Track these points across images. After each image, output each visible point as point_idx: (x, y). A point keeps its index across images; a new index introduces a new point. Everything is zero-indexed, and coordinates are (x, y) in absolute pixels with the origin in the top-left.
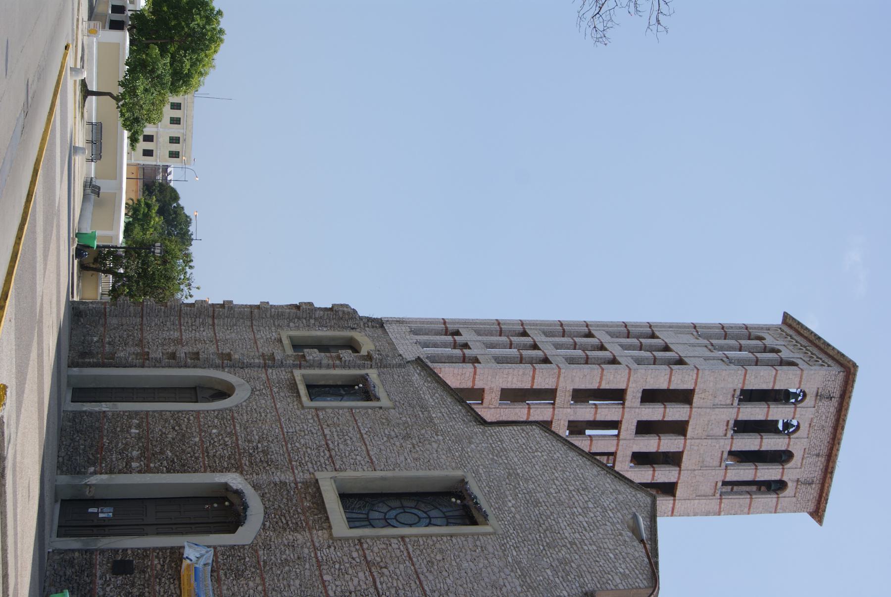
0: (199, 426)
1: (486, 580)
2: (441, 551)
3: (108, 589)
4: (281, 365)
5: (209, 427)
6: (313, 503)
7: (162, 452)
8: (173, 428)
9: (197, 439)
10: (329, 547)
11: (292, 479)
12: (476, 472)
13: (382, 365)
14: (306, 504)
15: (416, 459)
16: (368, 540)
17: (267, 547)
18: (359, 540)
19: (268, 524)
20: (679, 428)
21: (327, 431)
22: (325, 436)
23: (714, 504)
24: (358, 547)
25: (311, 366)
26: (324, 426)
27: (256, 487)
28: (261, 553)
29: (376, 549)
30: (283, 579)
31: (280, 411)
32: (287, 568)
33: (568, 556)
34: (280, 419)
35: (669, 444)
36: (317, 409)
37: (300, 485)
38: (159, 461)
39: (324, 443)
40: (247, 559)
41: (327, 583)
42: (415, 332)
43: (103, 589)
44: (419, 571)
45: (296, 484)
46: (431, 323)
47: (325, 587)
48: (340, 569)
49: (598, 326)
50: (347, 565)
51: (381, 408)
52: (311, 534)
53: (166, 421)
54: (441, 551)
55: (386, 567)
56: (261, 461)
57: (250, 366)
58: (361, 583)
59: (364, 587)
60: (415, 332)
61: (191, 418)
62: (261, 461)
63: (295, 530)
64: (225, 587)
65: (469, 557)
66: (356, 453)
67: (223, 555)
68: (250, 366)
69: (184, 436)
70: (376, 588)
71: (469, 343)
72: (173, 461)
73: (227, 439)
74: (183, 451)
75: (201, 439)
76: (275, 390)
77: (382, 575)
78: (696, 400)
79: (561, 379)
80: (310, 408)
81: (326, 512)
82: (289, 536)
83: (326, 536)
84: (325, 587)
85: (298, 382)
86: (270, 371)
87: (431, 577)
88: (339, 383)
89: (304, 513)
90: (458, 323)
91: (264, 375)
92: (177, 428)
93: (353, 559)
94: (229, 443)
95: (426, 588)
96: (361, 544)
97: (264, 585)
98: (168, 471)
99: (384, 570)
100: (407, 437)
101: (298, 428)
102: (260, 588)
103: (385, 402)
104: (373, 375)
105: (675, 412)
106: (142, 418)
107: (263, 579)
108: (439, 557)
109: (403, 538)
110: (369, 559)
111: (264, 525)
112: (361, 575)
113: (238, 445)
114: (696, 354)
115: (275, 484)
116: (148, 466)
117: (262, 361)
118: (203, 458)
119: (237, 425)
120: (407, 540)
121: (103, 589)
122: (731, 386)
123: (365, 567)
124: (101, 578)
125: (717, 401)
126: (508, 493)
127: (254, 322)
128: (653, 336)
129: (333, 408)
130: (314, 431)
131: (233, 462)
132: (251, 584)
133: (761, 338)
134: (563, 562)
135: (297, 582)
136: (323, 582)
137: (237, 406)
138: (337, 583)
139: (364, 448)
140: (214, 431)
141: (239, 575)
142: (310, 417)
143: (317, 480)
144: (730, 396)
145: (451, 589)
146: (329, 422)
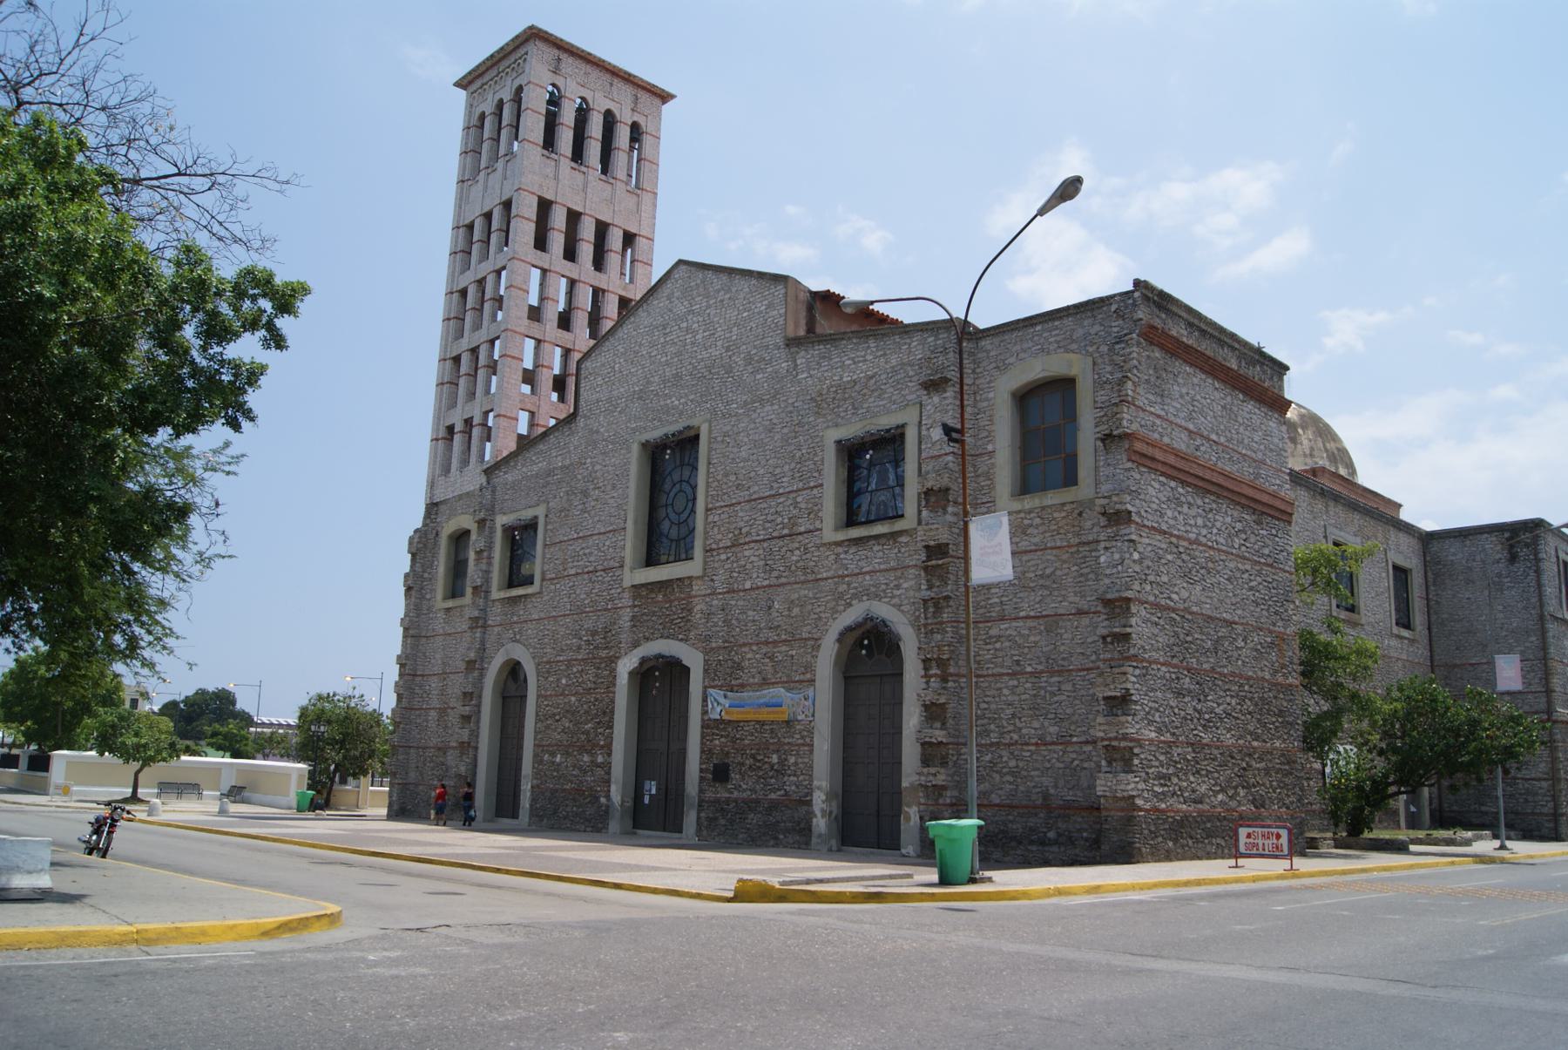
0: (556, 696)
1: (763, 436)
2: (726, 475)
3: (744, 787)
4: (484, 610)
6: (660, 592)
7: (587, 733)
8: (557, 721)
9: (573, 699)
10: (712, 580)
11: (628, 610)
12: (634, 430)
13: (491, 510)
14: (660, 597)
15: (614, 487)
16: (708, 543)
17: (708, 639)
18: (707, 551)
19: (680, 636)
20: (574, 217)
21: (573, 572)
22: (577, 574)
23: (646, 197)
24: (715, 553)
25: (487, 581)
26: (566, 574)
27: (636, 645)
28: (714, 645)
29: (720, 537)
30: (746, 626)
31: (542, 615)
32: (733, 622)
33: (742, 356)
34: (554, 617)
35: (587, 231)
36: (543, 579)
38: (597, 736)
39: (586, 576)
40: (721, 658)
41: (754, 586)
42: (446, 470)
43: (745, 790)
44: (747, 498)
45: (635, 606)
46: (435, 457)
47: (758, 588)
48: (739, 573)
49: (453, 281)
50: (735, 565)
51: (547, 516)
52: (695, 596)
53: (548, 727)
54: (726, 475)
55: (740, 529)
56: (604, 638)
57: (483, 642)
58: (756, 553)
59: (761, 552)
60: (446, 470)
61: (546, 703)
62: (604, 638)
63: (690, 611)
64: (751, 680)
65: (735, 450)
66: (601, 545)
68: (483, 642)
69: (567, 711)
70: (764, 540)
71: (466, 417)
72: (598, 723)
73: (575, 670)
74: (586, 712)
76: (515, 618)
77: (748, 533)
78: (549, 196)
79: (518, 329)
80: (541, 585)
81: (671, 580)
82: (697, 617)
83: (699, 582)
84: (758, 588)
85: (508, 595)
86: (490, 622)
87: (756, 488)
88: (509, 554)
90: (438, 424)
91: (496, 629)
92: (557, 717)
93: (728, 558)
94: (580, 668)
95: (767, 494)
96: (712, 550)
97: (751, 644)
98: (611, 727)
99: (744, 530)
100: (585, 493)
101: (566, 600)
102: (754, 648)
103: (540, 511)
104: (501, 520)
105: (559, 219)
106: (543, 751)
107: (744, 645)
108: (733, 478)
109: (707, 510)
110: (729, 544)
111: (681, 640)
112: (747, 553)
113: (583, 660)
114: (497, 187)
115: (634, 626)
116: (602, 747)
117: (479, 630)
119: (558, 658)
120: (710, 506)
121: (745, 790)
122: (539, 157)
123: (739, 549)
124: (732, 793)
125: (551, 175)
126: (662, 403)
127: (423, 634)
128: (470, 227)
129: (543, 563)
130: (571, 584)
131: (603, 665)
132: (749, 656)
133: (482, 117)
134: (749, 360)
135: (750, 613)
136: (752, 589)
137: (534, 658)
138: (755, 576)
139: (595, 538)
140: (564, 681)
141: (739, 667)
142: (553, 587)
143: (633, 586)
144: (548, 161)
145: (771, 470)
146: (561, 568)
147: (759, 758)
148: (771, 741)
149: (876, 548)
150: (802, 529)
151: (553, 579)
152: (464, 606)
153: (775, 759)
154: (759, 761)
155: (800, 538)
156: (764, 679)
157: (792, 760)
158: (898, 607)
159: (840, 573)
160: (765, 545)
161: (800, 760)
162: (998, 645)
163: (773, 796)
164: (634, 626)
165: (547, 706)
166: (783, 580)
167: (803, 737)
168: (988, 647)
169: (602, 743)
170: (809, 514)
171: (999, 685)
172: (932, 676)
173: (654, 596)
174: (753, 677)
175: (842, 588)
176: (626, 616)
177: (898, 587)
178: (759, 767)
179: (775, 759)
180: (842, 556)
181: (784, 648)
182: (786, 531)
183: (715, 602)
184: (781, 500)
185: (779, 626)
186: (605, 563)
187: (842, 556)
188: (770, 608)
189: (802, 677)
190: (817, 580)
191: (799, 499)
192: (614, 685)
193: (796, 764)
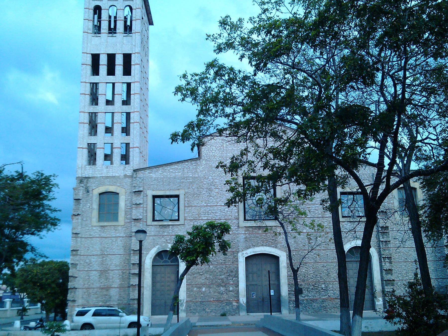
7: (222, 279)
21: (206, 218)
27: (248, 248)
37: (246, 233)
103: (181, 193)
106: (192, 287)
121: (310, 296)
147: (316, 286)
148: (321, 280)
151: (192, 220)
153: (323, 286)
154: (316, 287)
155: (327, 218)
156: (315, 261)
157: (331, 286)
162: (399, 254)
163: (323, 297)
168: (396, 254)
169: (231, 283)
171: (401, 265)
172: (386, 262)
174: (311, 260)
178: (316, 289)
179: (323, 286)
181: (324, 252)
182: (320, 216)
184: (317, 206)
186: (226, 217)
189: (332, 261)
192: (238, 261)
193: (332, 287)
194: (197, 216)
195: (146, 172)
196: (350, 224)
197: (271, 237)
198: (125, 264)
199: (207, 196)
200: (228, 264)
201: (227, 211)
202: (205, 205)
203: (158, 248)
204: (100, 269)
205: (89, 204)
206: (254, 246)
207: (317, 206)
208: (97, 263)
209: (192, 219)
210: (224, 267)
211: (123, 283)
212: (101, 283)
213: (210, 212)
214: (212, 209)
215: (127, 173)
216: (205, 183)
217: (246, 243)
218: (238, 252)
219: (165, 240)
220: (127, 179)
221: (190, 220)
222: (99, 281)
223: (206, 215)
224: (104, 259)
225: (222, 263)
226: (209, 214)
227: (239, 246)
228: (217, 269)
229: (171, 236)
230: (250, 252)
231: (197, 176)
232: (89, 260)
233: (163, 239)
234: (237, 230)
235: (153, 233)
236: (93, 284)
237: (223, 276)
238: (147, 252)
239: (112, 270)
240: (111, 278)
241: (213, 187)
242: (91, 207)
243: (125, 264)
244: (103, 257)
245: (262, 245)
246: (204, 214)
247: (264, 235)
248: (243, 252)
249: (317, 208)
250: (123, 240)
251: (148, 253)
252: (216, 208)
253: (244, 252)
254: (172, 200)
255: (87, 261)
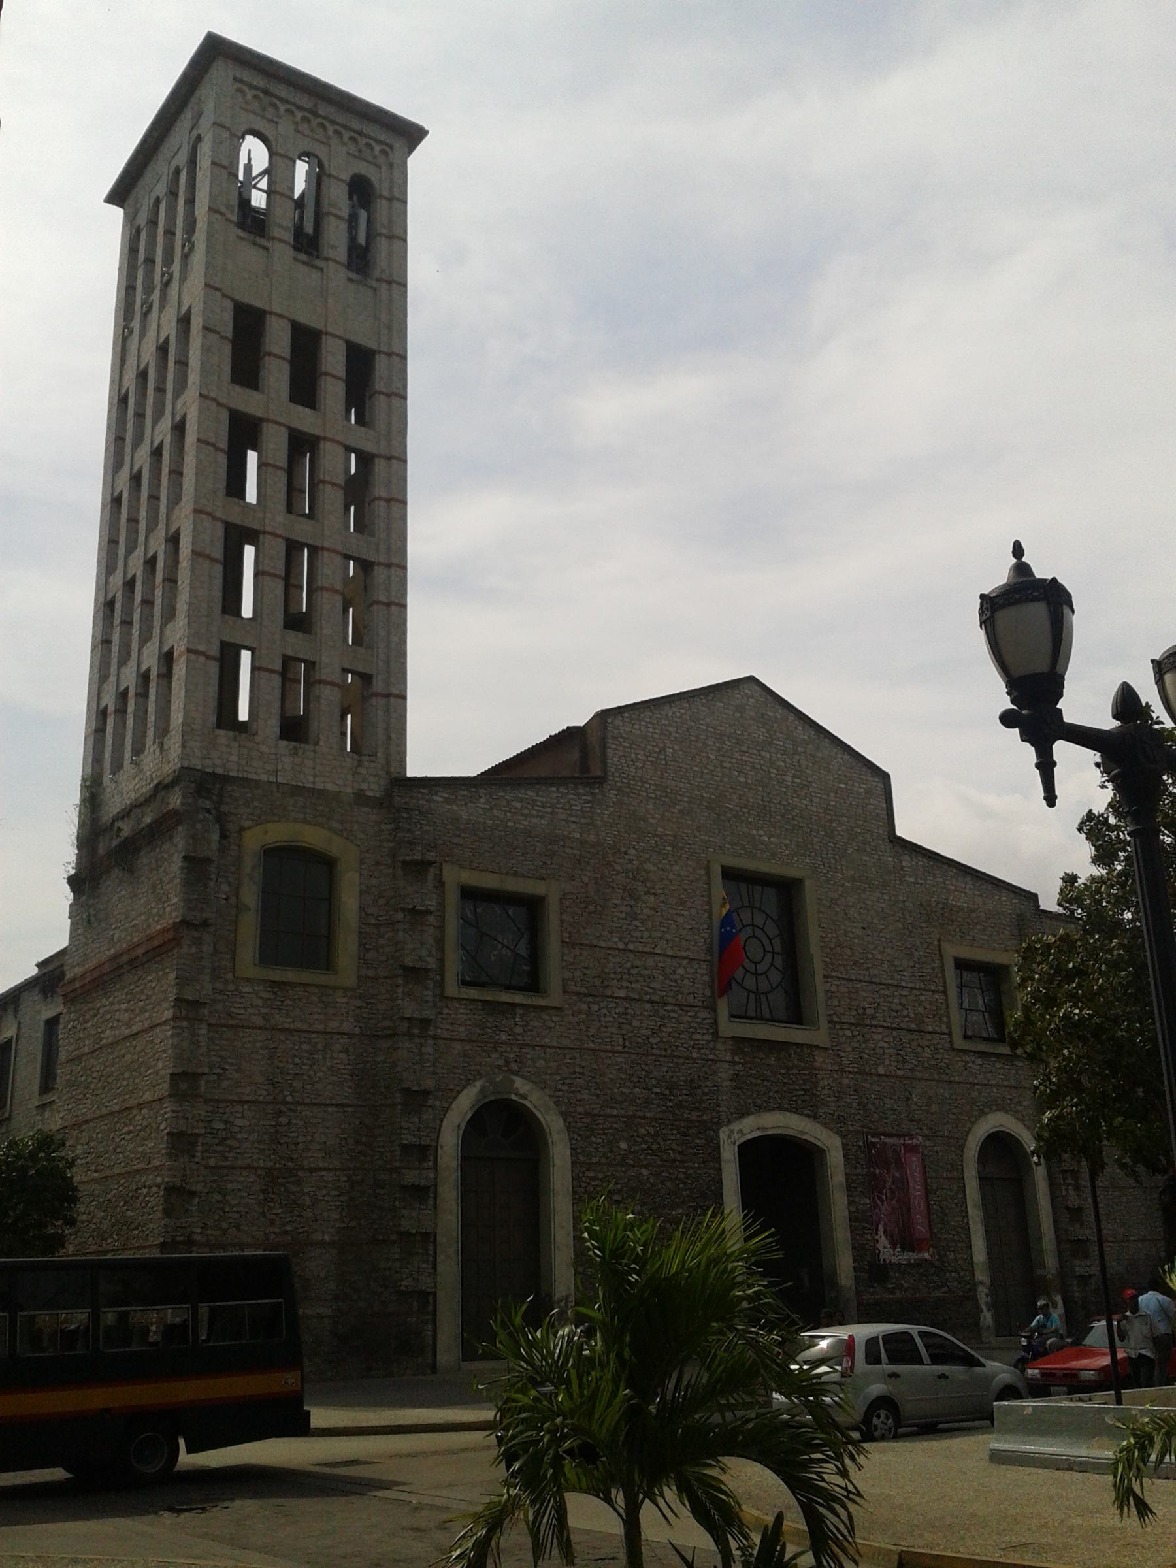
3: (906, 1285)
5: (611, 1151)
9: (645, 1172)
14: (772, 1061)
19: (806, 1112)
21: (622, 993)
27: (743, 1114)
29: (841, 1010)
32: (870, 1106)
37: (737, 1059)
43: (906, 1290)
61: (591, 1174)
67: (855, 1168)
75: (645, 1167)
77: (873, 1017)
89: (788, 1068)
111: (808, 1116)
112: (875, 1037)
113: (656, 1119)
115: (736, 1088)
118: (687, 1168)
119: (608, 1111)
123: (866, 1030)
124: (894, 1293)
142: (585, 1007)
143: (733, 1037)
149: (998, 1065)
150: (930, 1029)
152: (335, 988)
157: (952, 1257)
158: (1022, 1120)
159: (971, 1080)
160: (895, 1033)
161: (959, 1256)
163: (938, 1294)
164: (736, 1088)
165: (594, 1179)
166: (918, 1074)
167: (958, 1234)
170: (934, 1016)
173: (762, 1055)
175: (974, 1094)
176: (724, 1074)
177: (1019, 1103)
180: (970, 1065)
182: (913, 1026)
183: (846, 1081)
185: (920, 1120)
186: (680, 997)
187: (970, 1065)
188: (908, 1099)
189: (950, 1175)
190: (951, 1082)
191: (922, 998)
194: (597, 982)
195: (436, 794)
196: (979, 1061)
197: (801, 1082)
198: (360, 1148)
199: (623, 915)
200: (693, 1168)
201: (682, 978)
202: (621, 946)
203: (482, 1090)
204: (270, 1164)
205: (225, 888)
206: (760, 1109)
207: (905, 993)
208: (254, 1137)
209: (583, 990)
210: (681, 1176)
211: (352, 1224)
212: (272, 1222)
213: (634, 971)
214: (637, 963)
215: (364, 786)
216: (618, 867)
217: (738, 1096)
218: (719, 1125)
219: (501, 1062)
220: (366, 809)
221: (578, 994)
222: (264, 1214)
223: (625, 984)
224: (283, 1120)
225: (675, 1161)
226: (633, 979)
227: (719, 1106)
228: (663, 1183)
229: (521, 1046)
230: (751, 1127)
231: (592, 838)
232: (226, 1122)
233: (494, 1055)
234: (711, 1045)
235: (462, 1029)
236: (238, 1227)
237: (680, 1211)
238: (446, 1105)
239: (311, 1170)
240: (308, 1200)
241: (641, 889)
242: (233, 900)
243: (360, 1148)
244: (280, 1113)
245: (780, 1108)
246: (618, 977)
247: (783, 1071)
248: (732, 1127)
249: (904, 1001)
250: (351, 1049)
251: (448, 1108)
252: (650, 962)
253: (736, 1126)
254: (510, 912)
255: (218, 1125)
